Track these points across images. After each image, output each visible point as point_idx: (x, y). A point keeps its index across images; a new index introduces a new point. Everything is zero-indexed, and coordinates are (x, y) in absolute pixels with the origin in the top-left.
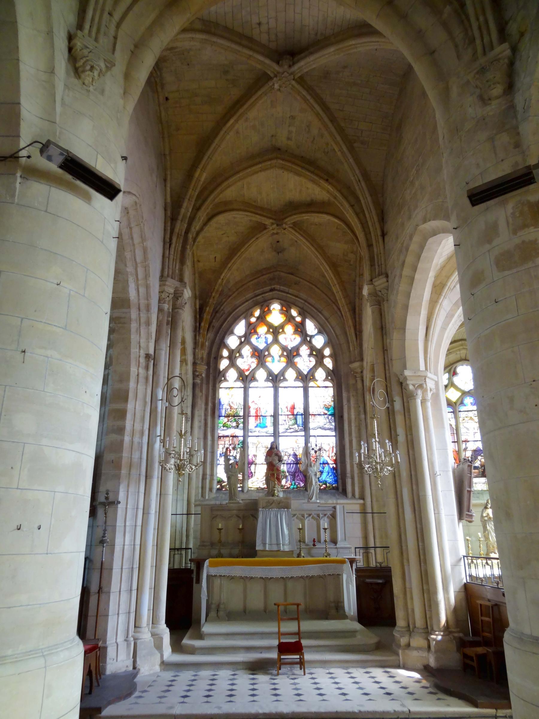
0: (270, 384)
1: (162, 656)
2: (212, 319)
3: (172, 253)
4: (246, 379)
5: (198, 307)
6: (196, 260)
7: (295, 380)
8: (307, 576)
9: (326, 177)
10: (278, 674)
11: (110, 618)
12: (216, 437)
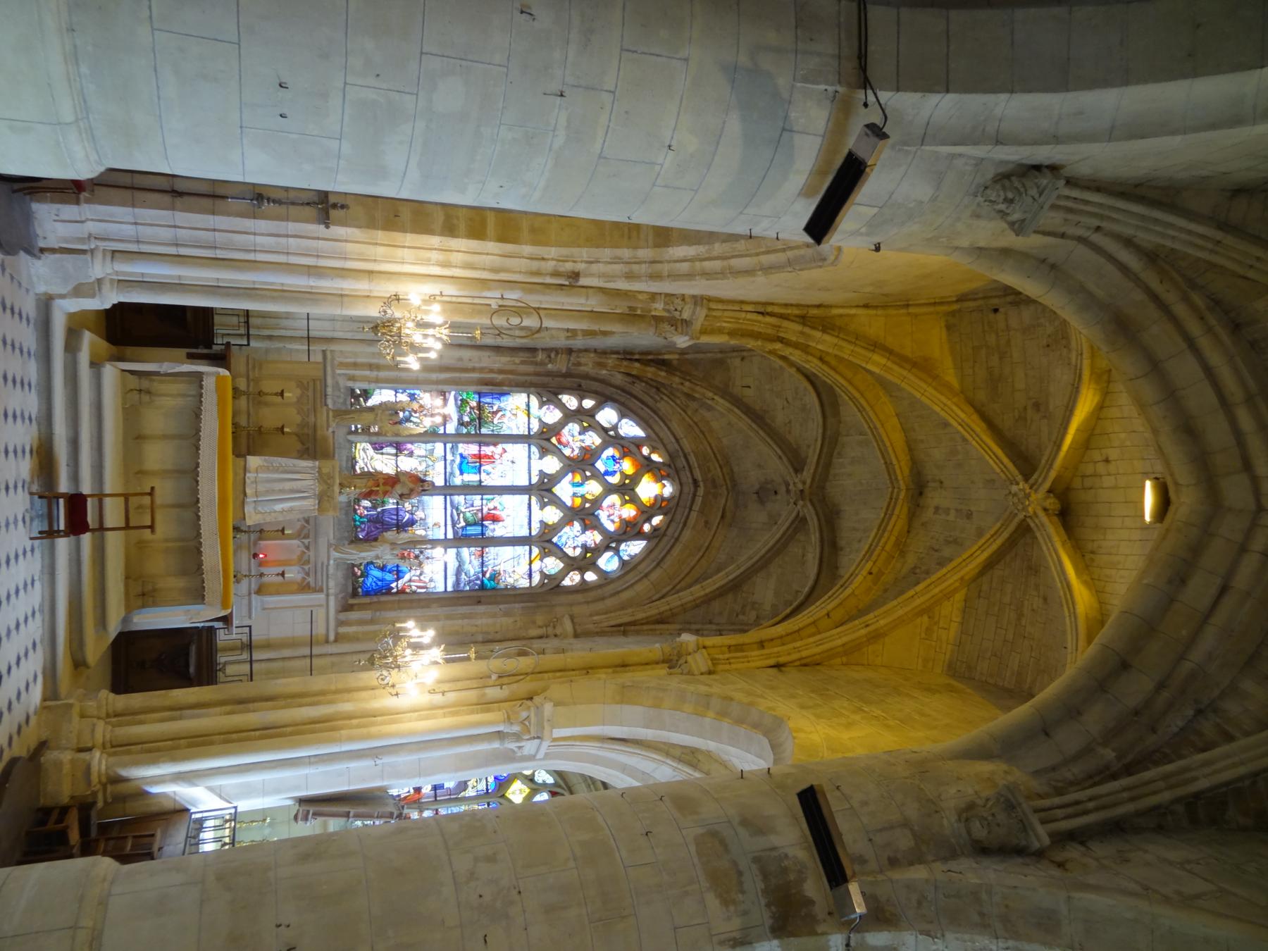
0: (535, 480)
1: (63, 297)
3: (749, 316)
4: (545, 439)
5: (666, 357)
6: (745, 354)
7: (541, 522)
8: (201, 543)
9: (875, 570)
10: (31, 494)
11: (130, 210)
12: (445, 388)
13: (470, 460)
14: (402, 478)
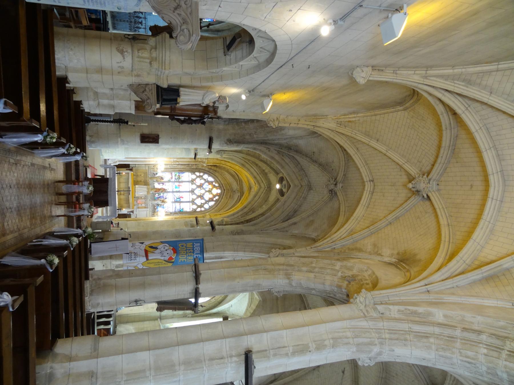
2: (213, 169)
4: (192, 181)
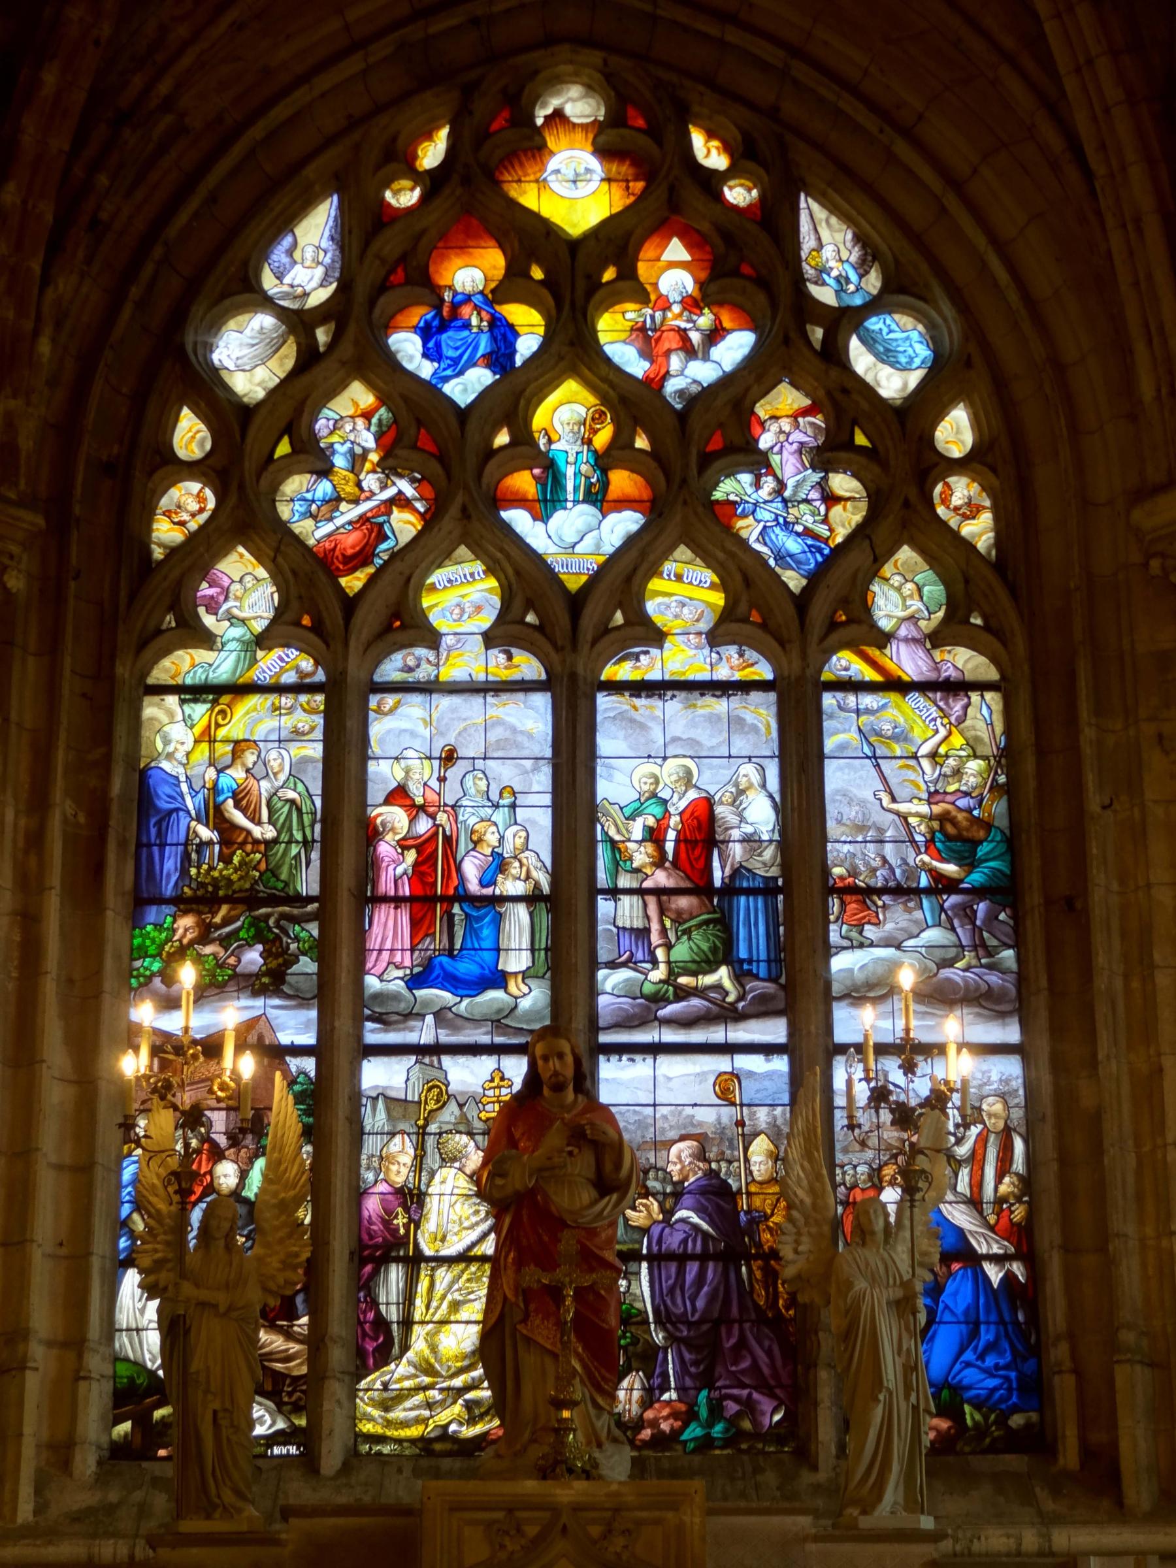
0: (528, 666)
4: (348, 628)
13: (439, 941)
14: (518, 1180)
